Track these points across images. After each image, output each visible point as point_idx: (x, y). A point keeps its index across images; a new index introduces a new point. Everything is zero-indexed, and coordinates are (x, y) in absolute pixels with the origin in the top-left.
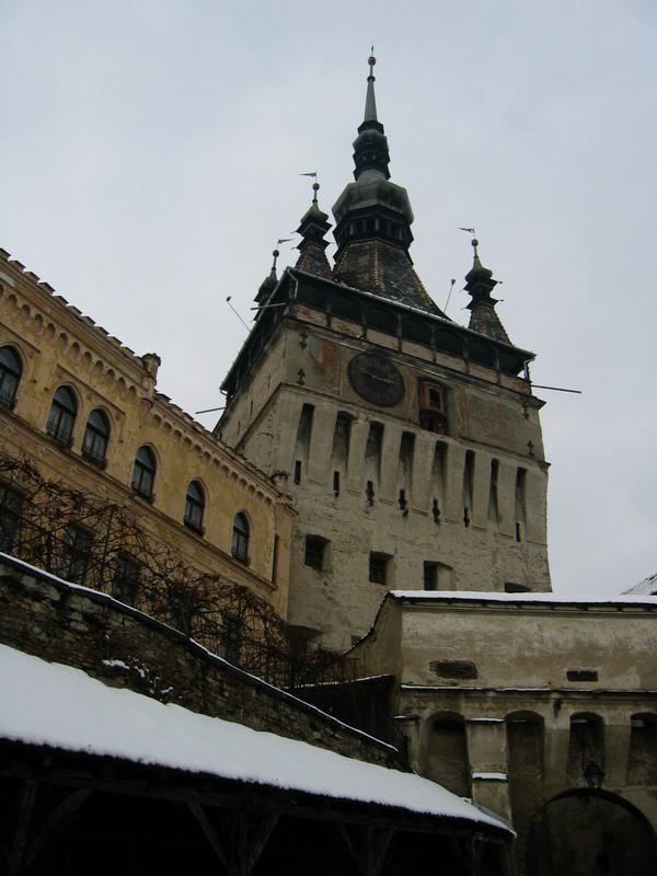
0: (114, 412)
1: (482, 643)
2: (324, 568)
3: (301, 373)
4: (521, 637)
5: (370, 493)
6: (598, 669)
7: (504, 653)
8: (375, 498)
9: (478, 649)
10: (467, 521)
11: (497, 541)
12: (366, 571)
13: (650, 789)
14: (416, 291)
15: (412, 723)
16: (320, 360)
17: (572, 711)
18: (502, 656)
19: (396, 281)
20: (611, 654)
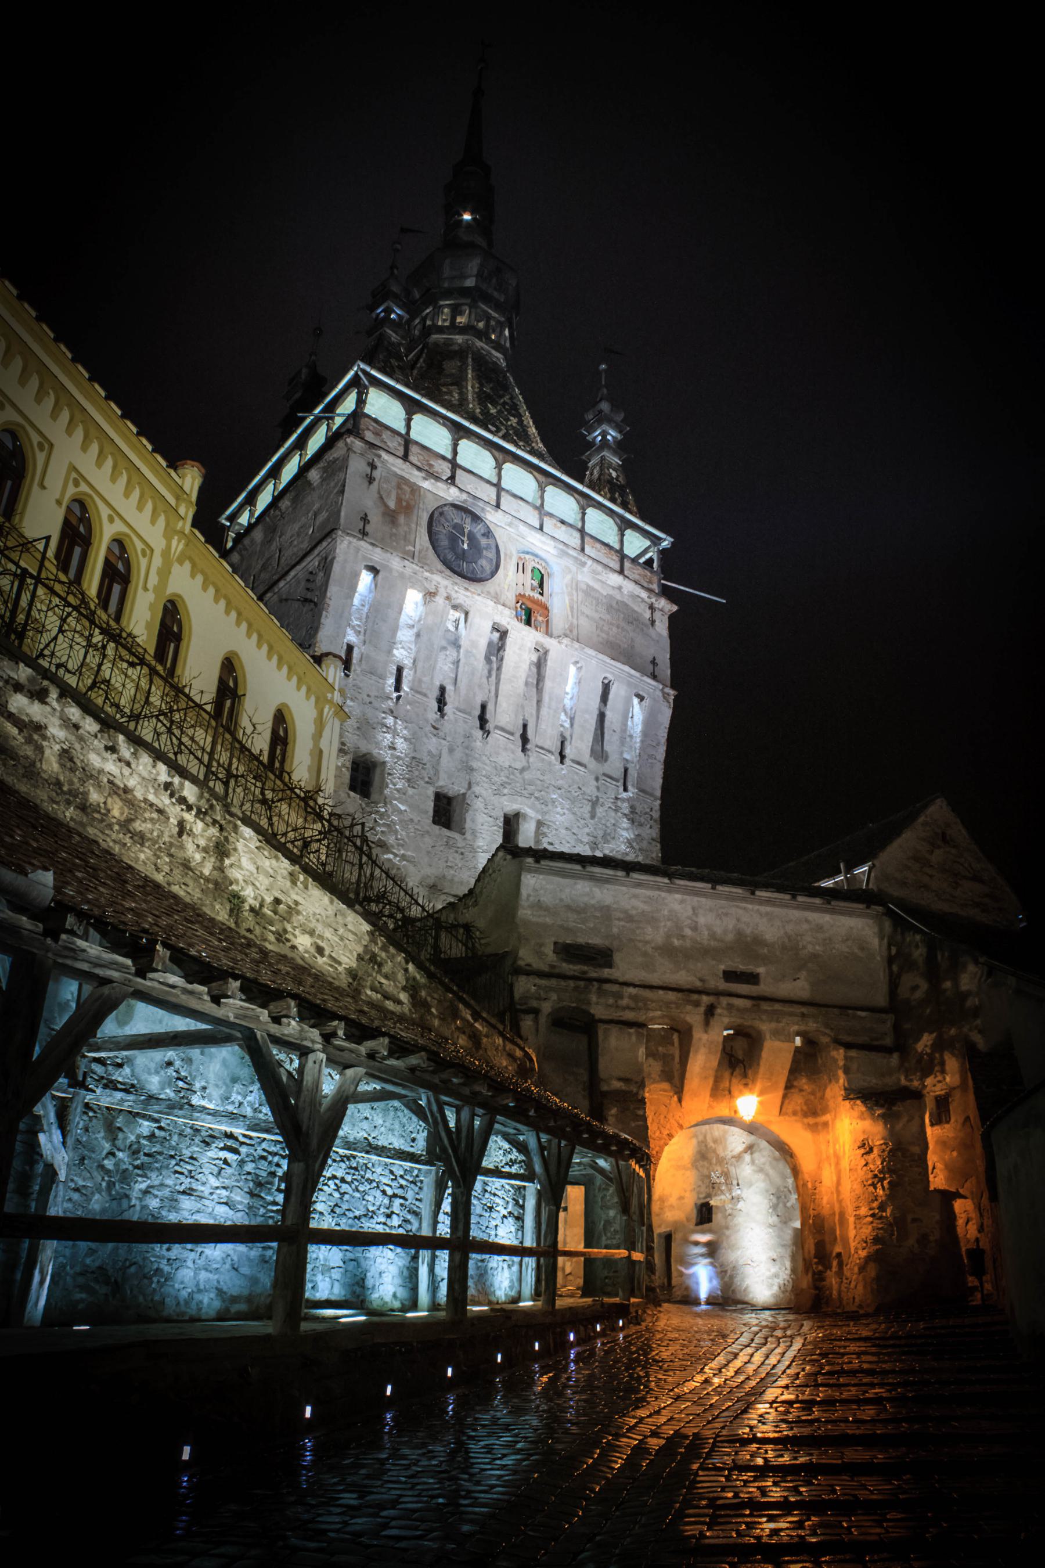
0: (139, 546)
1: (622, 923)
2: (374, 796)
3: (365, 519)
4: (669, 920)
5: (441, 701)
6: (761, 970)
7: (648, 938)
8: (447, 709)
9: (615, 930)
10: (562, 757)
11: (598, 788)
12: (430, 806)
13: (806, 1120)
14: (520, 422)
15: (531, 1016)
16: (392, 504)
17: (726, 1020)
18: (647, 942)
19: (494, 405)
20: (778, 953)
